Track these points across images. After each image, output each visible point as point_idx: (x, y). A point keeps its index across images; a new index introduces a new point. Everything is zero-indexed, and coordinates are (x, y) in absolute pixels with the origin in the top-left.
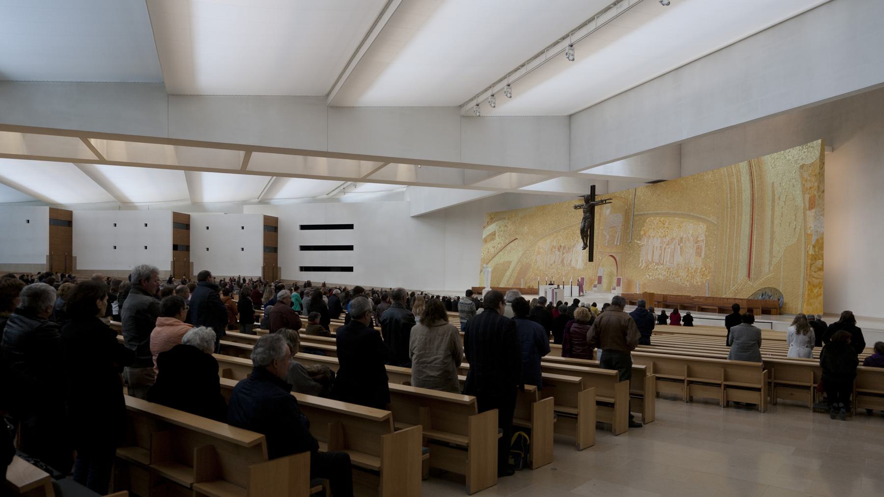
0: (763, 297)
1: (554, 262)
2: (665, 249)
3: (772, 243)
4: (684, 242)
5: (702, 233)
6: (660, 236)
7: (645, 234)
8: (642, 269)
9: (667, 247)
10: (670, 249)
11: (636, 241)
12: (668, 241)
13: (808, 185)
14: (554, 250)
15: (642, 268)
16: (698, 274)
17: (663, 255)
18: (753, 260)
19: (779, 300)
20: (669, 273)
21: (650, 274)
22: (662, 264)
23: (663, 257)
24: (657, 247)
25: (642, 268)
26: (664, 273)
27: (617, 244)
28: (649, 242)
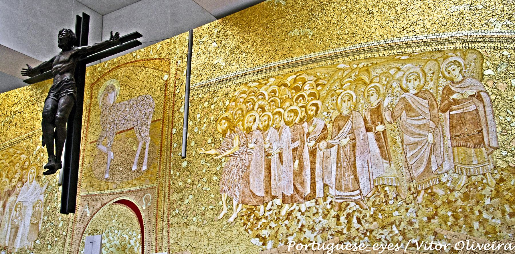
2: (313, 153)
5: (464, 78)
6: (287, 123)
7: (232, 128)
9: (323, 144)
10: (334, 150)
11: (202, 151)
22: (312, 196)
24: (280, 154)
26: (324, 222)
28: (251, 145)
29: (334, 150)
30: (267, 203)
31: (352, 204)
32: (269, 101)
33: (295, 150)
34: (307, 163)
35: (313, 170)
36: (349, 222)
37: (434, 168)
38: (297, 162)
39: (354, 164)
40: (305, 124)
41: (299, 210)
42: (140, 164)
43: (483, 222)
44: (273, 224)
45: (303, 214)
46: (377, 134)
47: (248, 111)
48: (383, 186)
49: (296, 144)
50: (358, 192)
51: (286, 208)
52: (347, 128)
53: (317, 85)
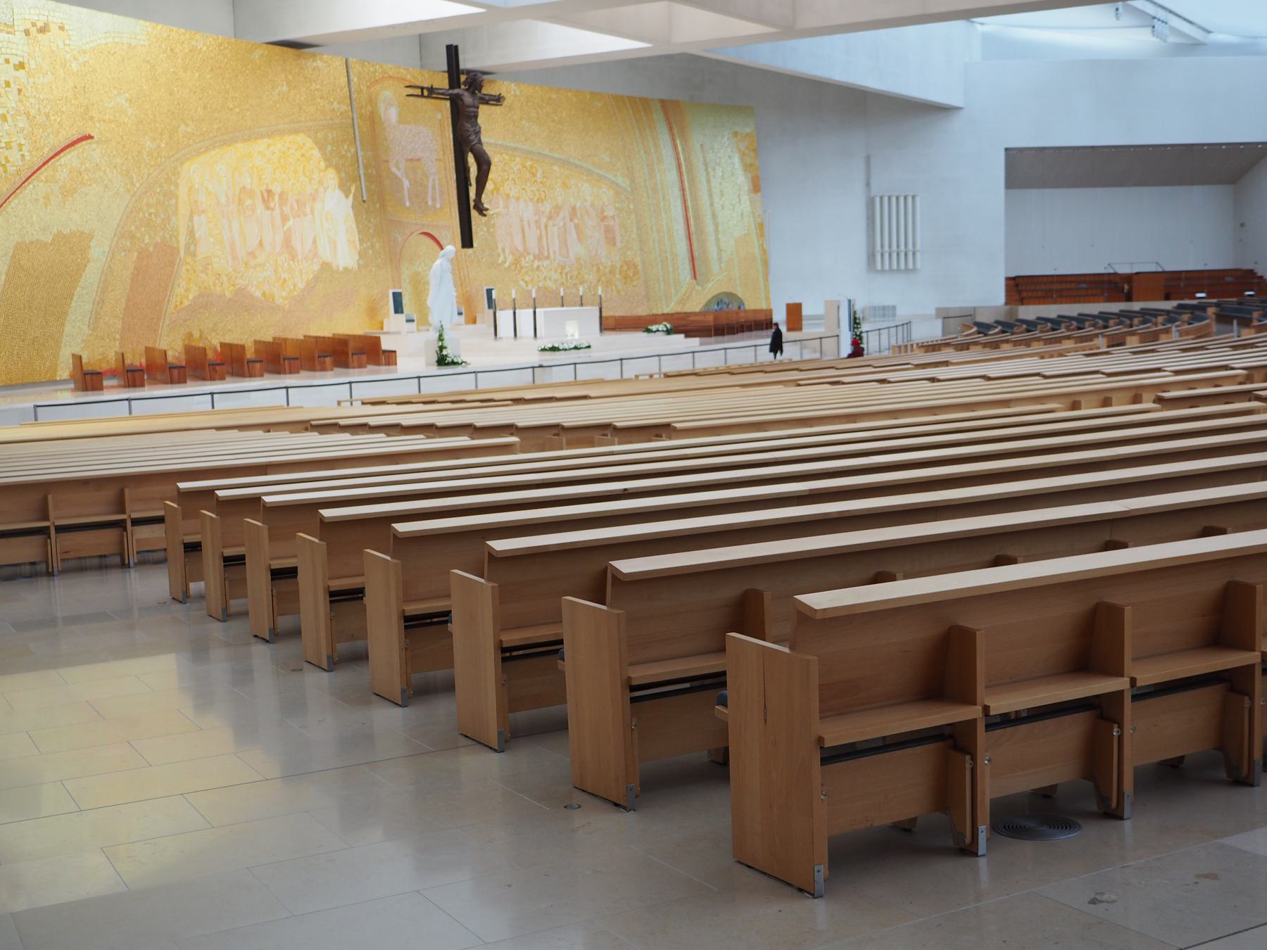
0: (720, 306)
1: (261, 244)
2: (546, 227)
3: (717, 231)
4: (579, 215)
6: (531, 200)
8: (509, 266)
9: (551, 223)
10: (556, 228)
12: (550, 212)
13: (748, 161)
14: (248, 202)
15: (507, 265)
16: (617, 276)
17: (544, 239)
18: (696, 254)
19: (739, 308)
20: (564, 275)
21: (527, 278)
22: (548, 258)
23: (545, 244)
24: (529, 224)
25: (507, 265)
27: (434, 206)
28: (511, 210)
29: (556, 228)
30: (525, 257)
31: (567, 267)
32: (519, 176)
33: (536, 221)
34: (544, 234)
35: (547, 239)
36: (567, 278)
37: (599, 253)
38: (538, 231)
39: (566, 241)
40: (540, 204)
41: (543, 266)
42: (434, 199)
43: (616, 286)
44: (530, 273)
45: (545, 268)
46: (575, 224)
47: (506, 180)
48: (579, 259)
49: (537, 218)
50: (568, 260)
51: (536, 264)
52: (561, 215)
53: (544, 177)
